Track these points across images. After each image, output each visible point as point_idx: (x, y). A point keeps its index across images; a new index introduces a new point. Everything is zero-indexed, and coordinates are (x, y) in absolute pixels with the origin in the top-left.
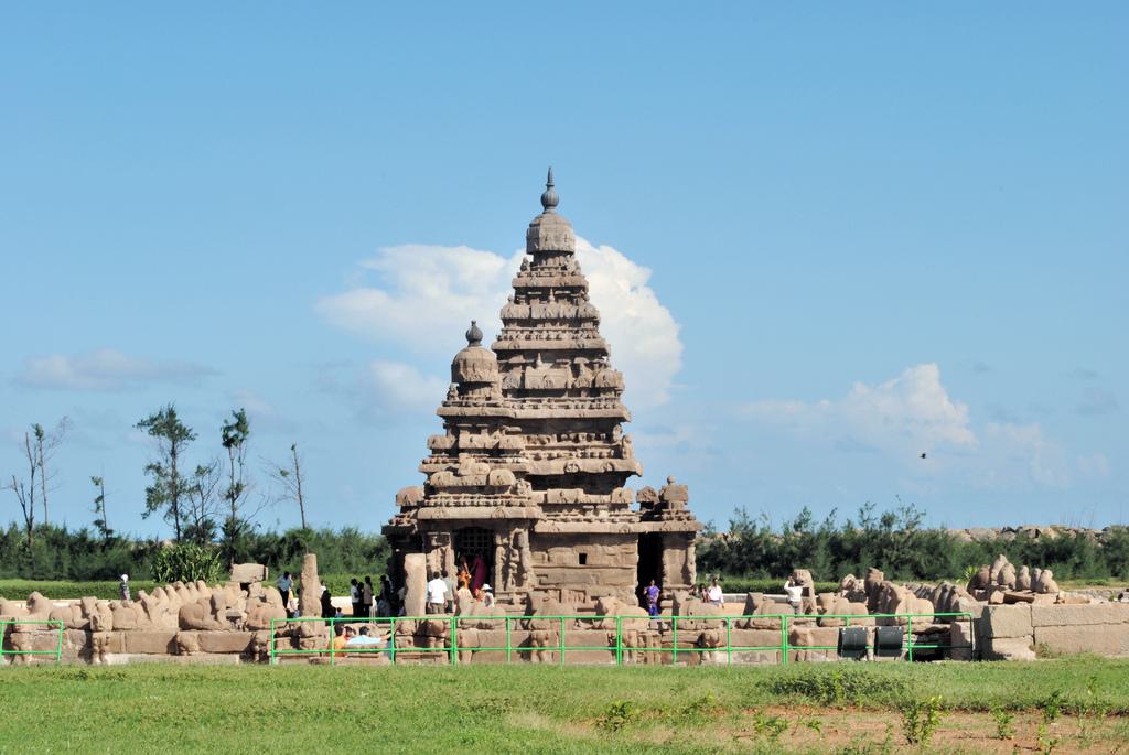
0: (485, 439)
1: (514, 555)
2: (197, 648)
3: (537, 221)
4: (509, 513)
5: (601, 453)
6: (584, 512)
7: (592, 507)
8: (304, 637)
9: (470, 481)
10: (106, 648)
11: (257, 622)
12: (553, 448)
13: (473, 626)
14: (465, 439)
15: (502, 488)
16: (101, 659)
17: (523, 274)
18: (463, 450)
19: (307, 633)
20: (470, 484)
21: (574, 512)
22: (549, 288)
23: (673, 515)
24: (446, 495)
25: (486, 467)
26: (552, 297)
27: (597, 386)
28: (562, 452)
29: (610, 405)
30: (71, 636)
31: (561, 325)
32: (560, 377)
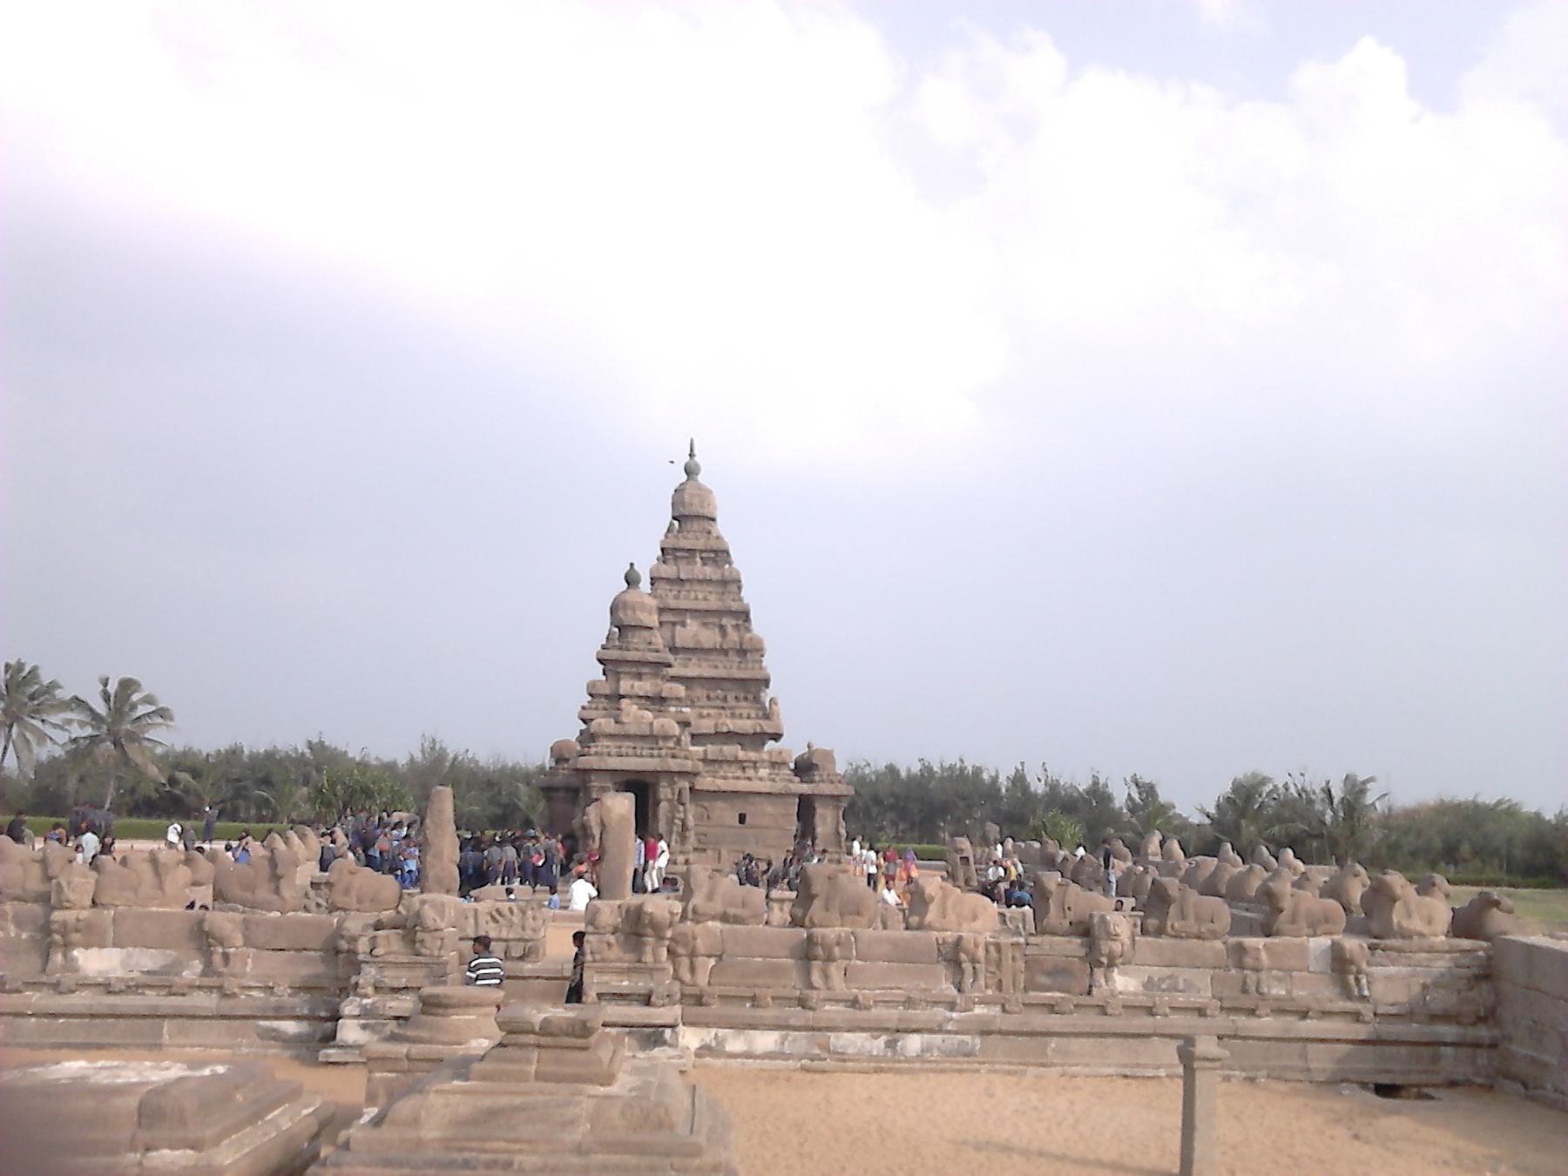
0: (645, 686)
1: (679, 812)
2: (240, 942)
4: (673, 765)
5: (749, 714)
6: (744, 768)
9: (632, 730)
12: (703, 707)
13: (713, 918)
14: (625, 685)
15: (666, 738)
16: (65, 956)
18: (623, 697)
19: (430, 923)
21: (733, 768)
23: (825, 777)
24: (606, 743)
25: (649, 715)
28: (712, 712)
32: (710, 637)
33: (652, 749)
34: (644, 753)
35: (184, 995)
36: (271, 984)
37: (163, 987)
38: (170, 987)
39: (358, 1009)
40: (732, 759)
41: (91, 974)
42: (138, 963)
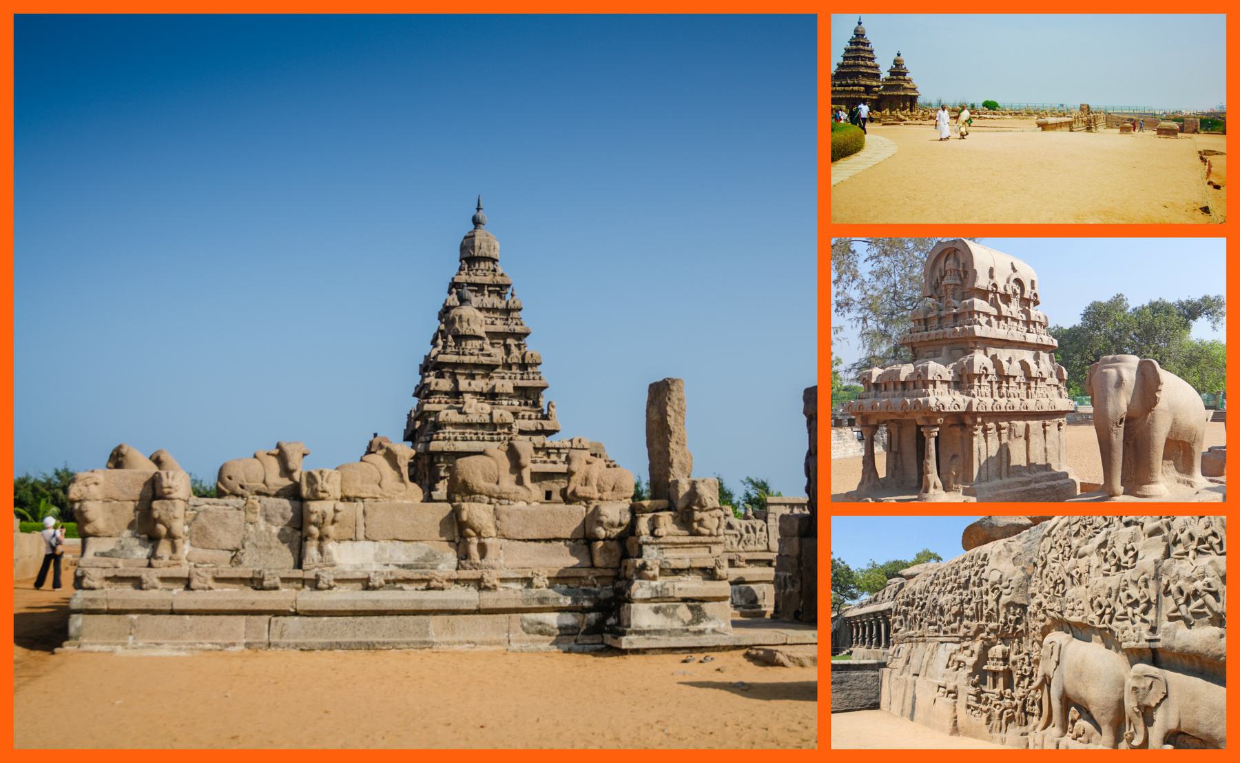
0: (480, 384)
2: (493, 533)
3: (472, 234)
5: (530, 416)
6: (548, 455)
7: (556, 451)
8: (702, 508)
9: (475, 418)
10: (331, 529)
11: (588, 489)
15: (503, 425)
16: (321, 550)
17: (462, 272)
20: (474, 421)
22: (483, 285)
25: (487, 407)
26: (486, 292)
27: (526, 362)
29: (537, 377)
30: (264, 509)
31: (493, 313)
33: (492, 434)
34: (486, 438)
35: (443, 589)
36: (530, 575)
37: (423, 580)
38: (429, 581)
39: (650, 591)
40: (540, 446)
41: (348, 569)
42: (391, 556)
